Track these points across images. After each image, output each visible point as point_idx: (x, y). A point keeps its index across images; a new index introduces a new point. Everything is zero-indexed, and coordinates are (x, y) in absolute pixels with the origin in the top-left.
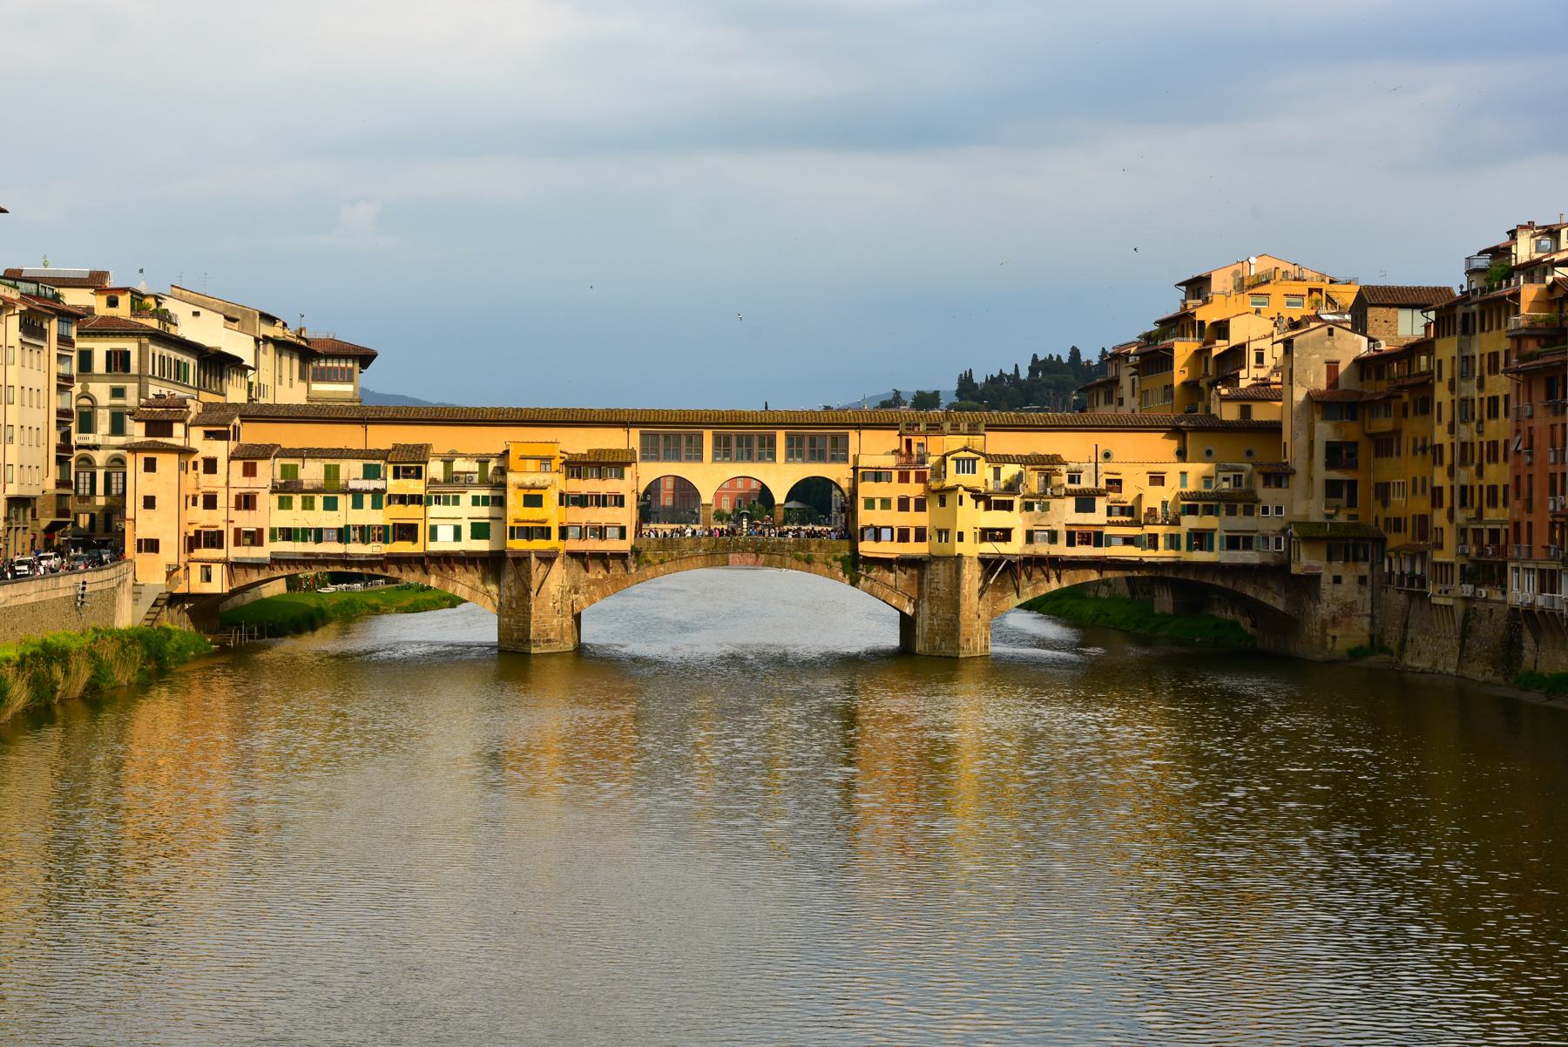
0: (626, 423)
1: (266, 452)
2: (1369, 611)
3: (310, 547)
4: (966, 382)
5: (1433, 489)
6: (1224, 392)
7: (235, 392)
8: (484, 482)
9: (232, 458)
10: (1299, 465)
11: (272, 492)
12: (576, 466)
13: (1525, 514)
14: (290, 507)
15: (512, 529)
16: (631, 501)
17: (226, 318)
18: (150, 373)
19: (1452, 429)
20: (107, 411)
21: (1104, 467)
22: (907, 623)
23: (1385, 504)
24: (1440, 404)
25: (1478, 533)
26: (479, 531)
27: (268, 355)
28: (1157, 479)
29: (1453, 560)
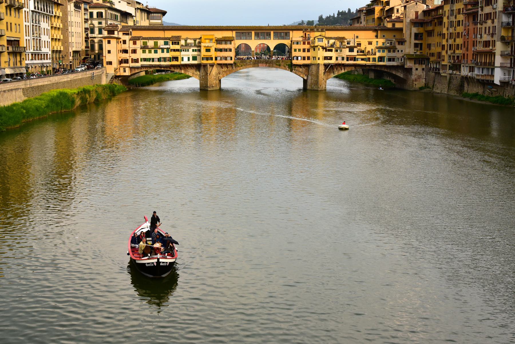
1: (139, 38)
2: (425, 77)
3: (151, 63)
4: (321, 18)
5: (442, 45)
6: (388, 20)
7: (130, 23)
8: (195, 46)
9: (130, 40)
11: (141, 49)
12: (219, 41)
14: (145, 53)
15: (203, 58)
16: (233, 50)
17: (127, 3)
18: (108, 18)
19: (448, 29)
20: (98, 28)
21: (356, 40)
22: (305, 82)
23: (430, 49)
24: (445, 23)
25: (454, 57)
26: (194, 58)
28: (370, 43)
29: (447, 64)
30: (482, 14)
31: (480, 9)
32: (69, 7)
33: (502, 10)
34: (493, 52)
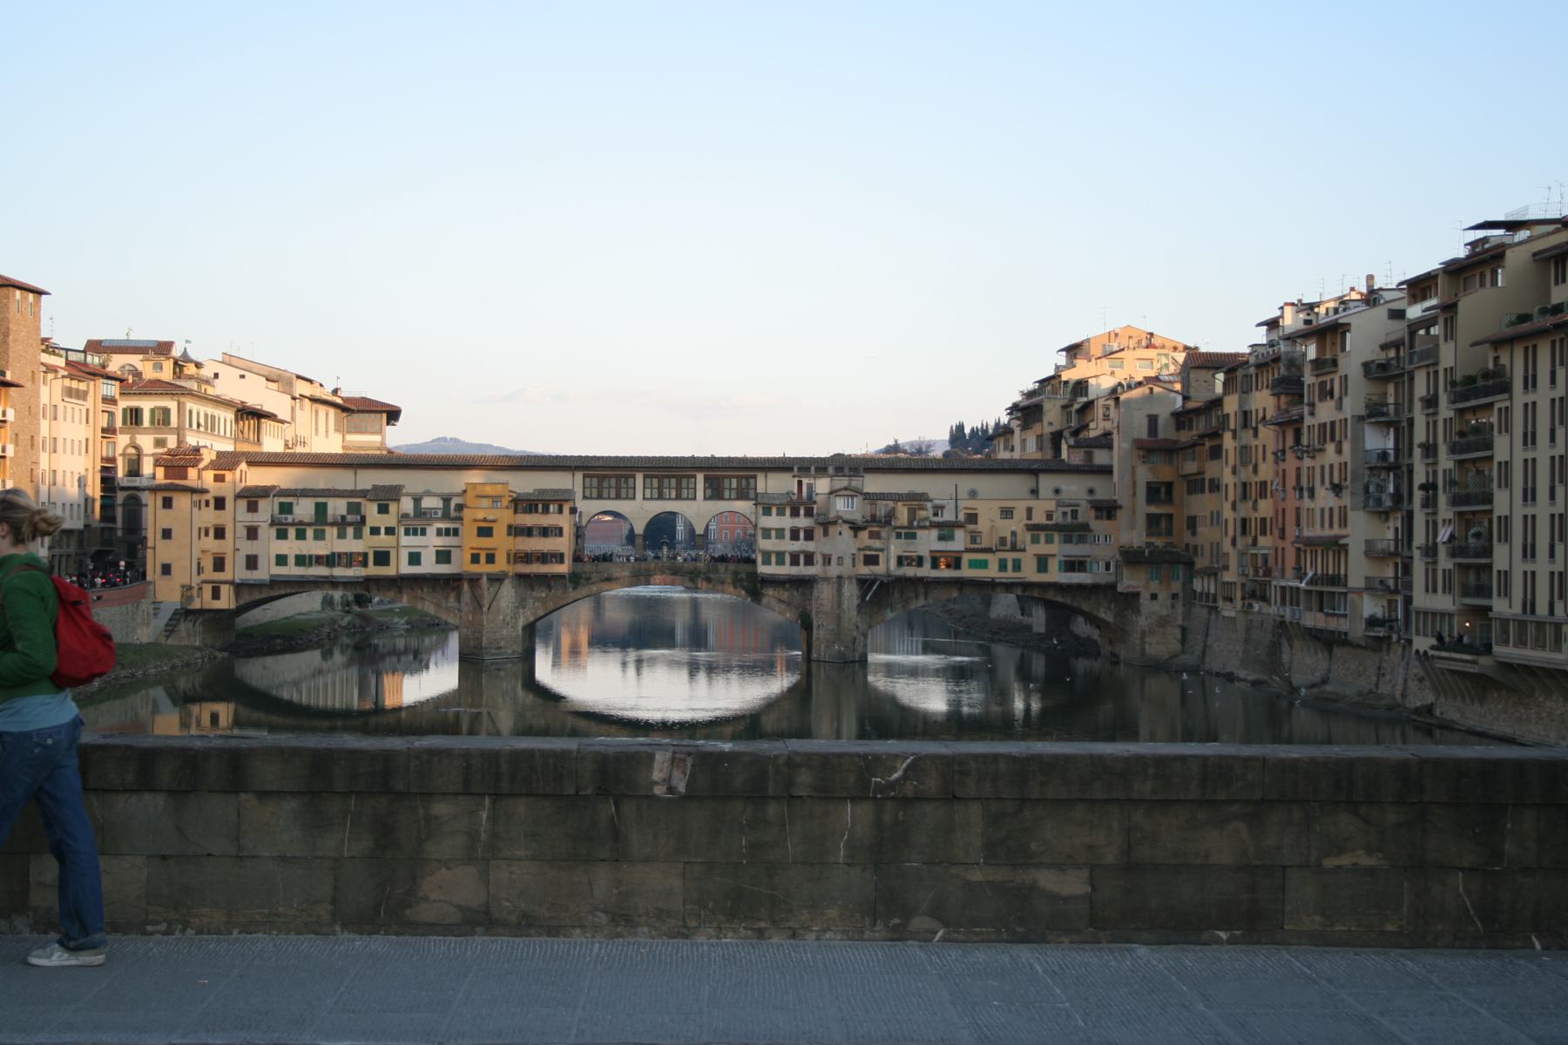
0: (571, 467)
1: (265, 492)
2: (1180, 622)
4: (957, 435)
8: (446, 516)
9: (238, 496)
12: (525, 504)
13: (1280, 541)
17: (267, 380)
18: (187, 426)
19: (1234, 472)
23: (1194, 533)
24: (1227, 450)
27: (306, 412)
28: (1007, 513)
30: (1314, 426)
31: (1306, 409)
32: (44, 391)
33: (1363, 412)
34: (1342, 542)
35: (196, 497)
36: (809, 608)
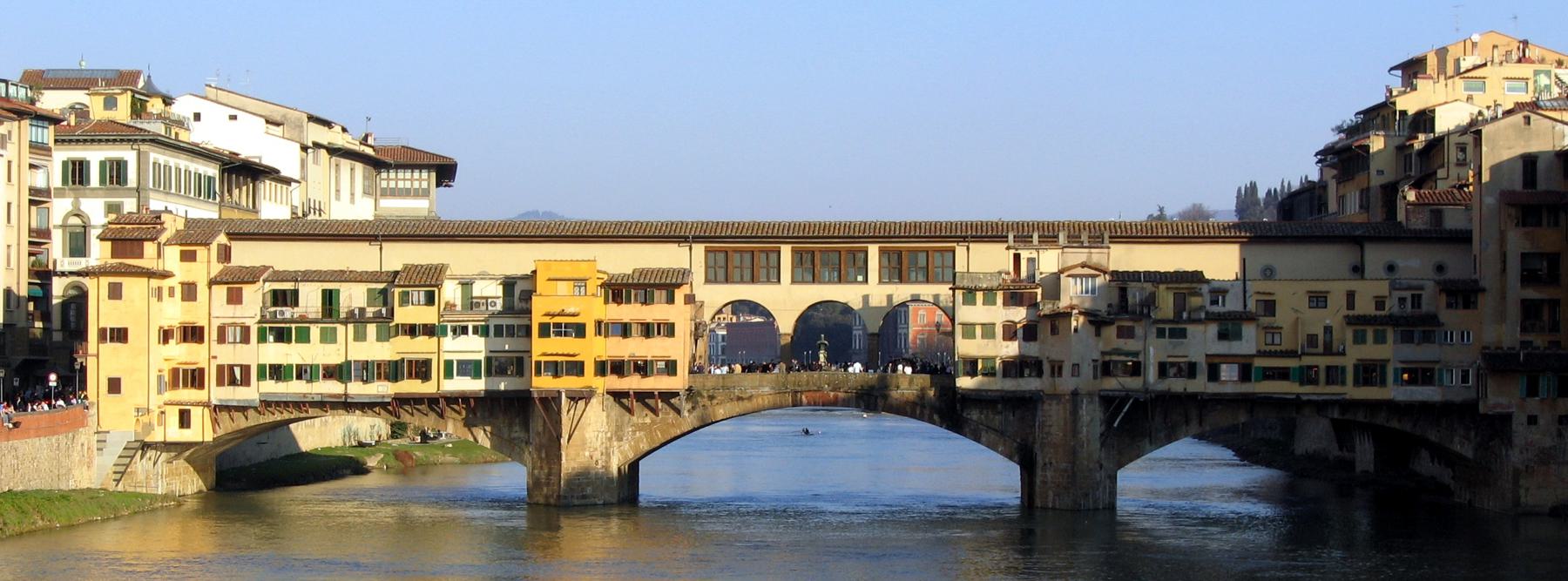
1: (252, 275)
4: (1247, 197)
7: (273, 206)
10: (1488, 278)
12: (617, 291)
16: (684, 328)
17: (267, 122)
18: (151, 186)
35: (155, 283)
36: (1031, 439)
